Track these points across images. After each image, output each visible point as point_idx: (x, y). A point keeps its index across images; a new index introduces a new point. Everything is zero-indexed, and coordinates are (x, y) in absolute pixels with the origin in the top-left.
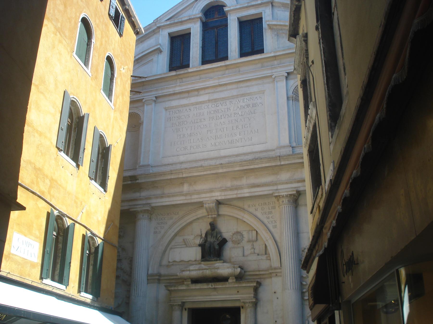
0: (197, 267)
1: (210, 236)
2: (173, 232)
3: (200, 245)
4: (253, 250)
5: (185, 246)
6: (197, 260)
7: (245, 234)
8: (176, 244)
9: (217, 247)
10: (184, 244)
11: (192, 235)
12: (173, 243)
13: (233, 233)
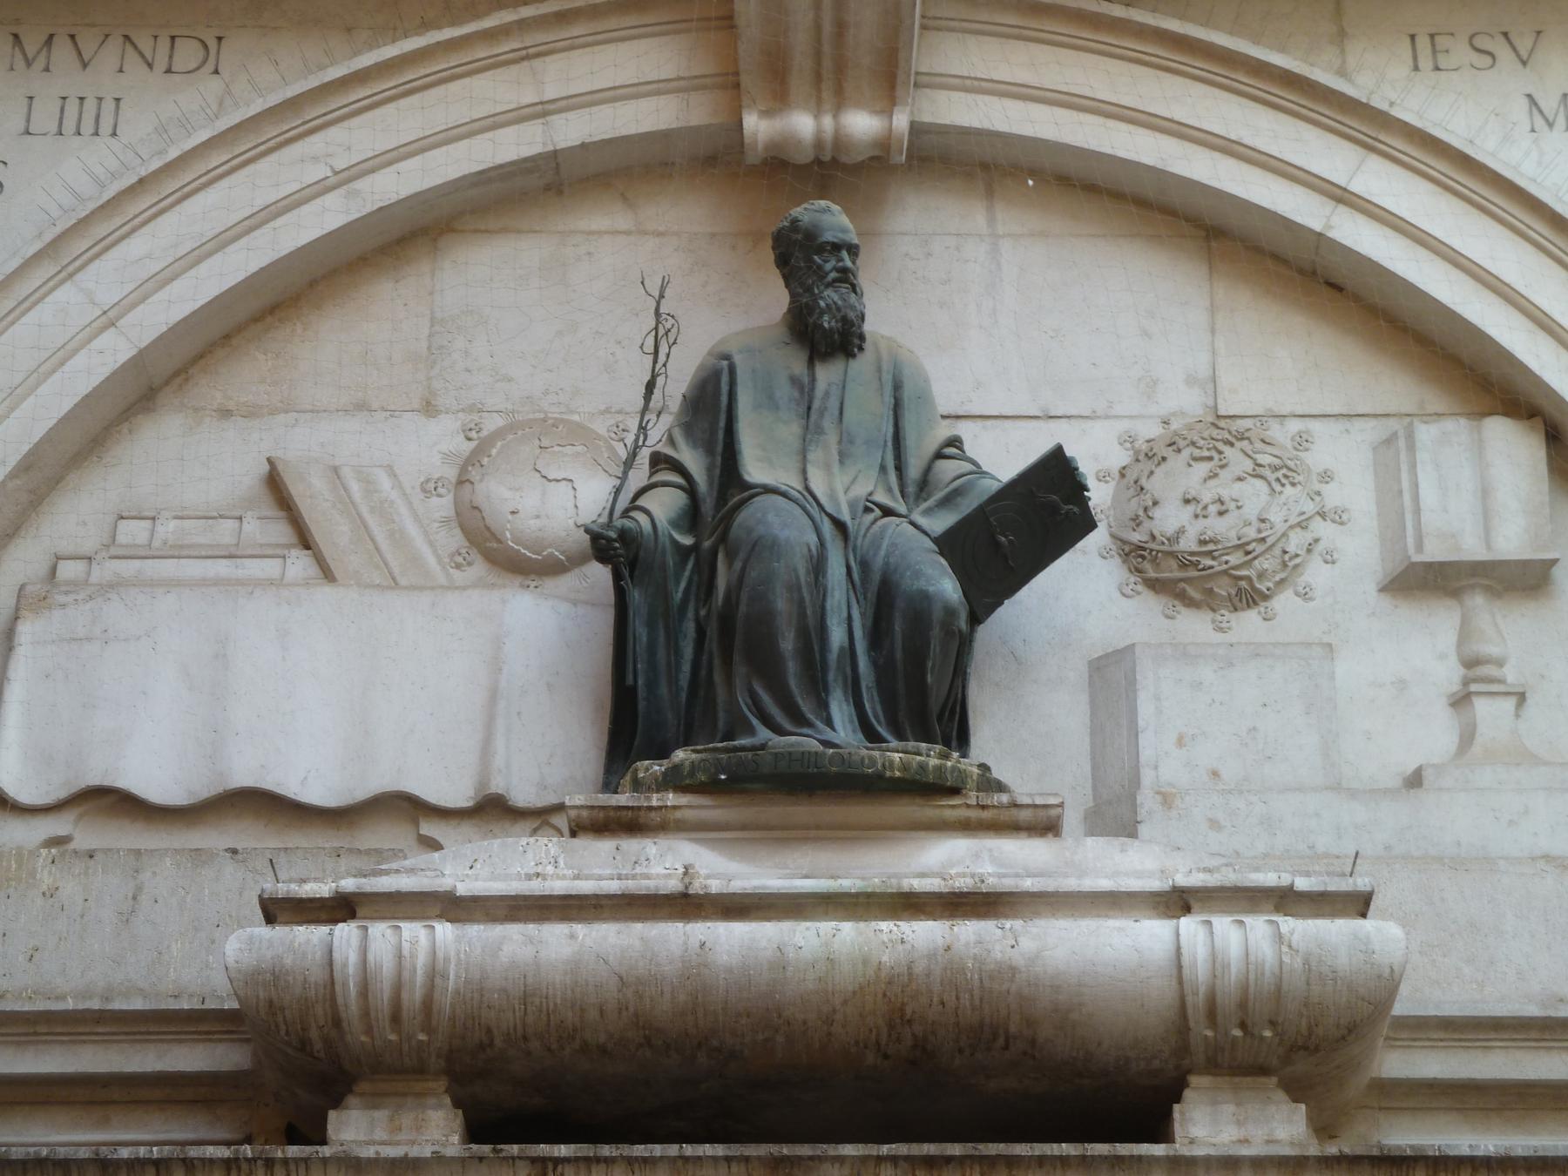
0: (599, 865)
1: (790, 430)
2: (109, 320)
3: (615, 547)
4: (1491, 713)
5: (299, 564)
6: (523, 795)
7: (1344, 462)
8: (133, 532)
9: (947, 587)
10: (280, 532)
11: (429, 408)
12: (74, 519)
13: (1150, 430)
